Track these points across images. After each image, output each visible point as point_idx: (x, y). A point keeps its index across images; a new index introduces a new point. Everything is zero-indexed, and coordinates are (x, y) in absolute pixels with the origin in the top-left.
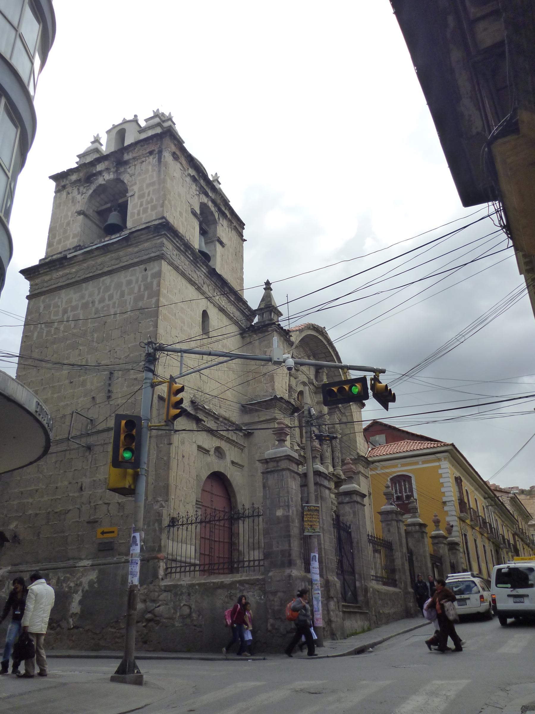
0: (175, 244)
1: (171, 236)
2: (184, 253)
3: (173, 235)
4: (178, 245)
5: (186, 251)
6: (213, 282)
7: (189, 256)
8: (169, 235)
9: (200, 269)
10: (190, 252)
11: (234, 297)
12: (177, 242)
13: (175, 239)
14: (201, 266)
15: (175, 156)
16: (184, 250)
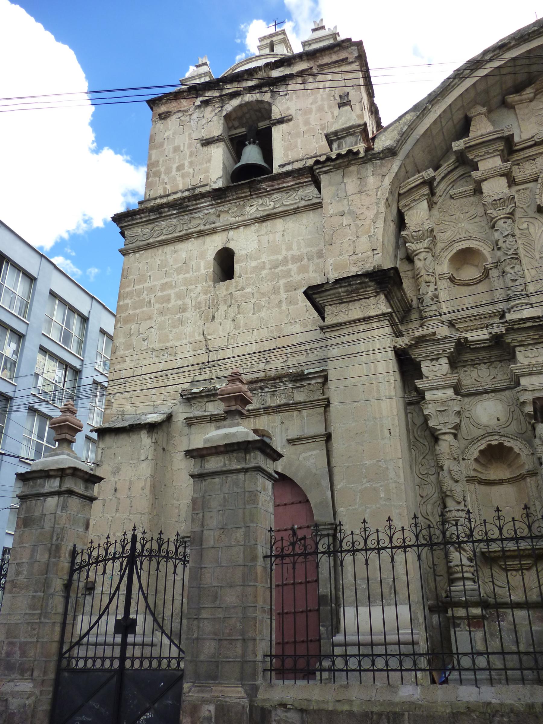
0: (142, 222)
1: (129, 221)
2: (161, 217)
3: (130, 218)
4: (145, 219)
5: (161, 213)
6: (234, 199)
7: (170, 213)
8: (125, 224)
9: (200, 208)
10: (166, 210)
11: (290, 179)
12: (141, 218)
13: (136, 219)
14: (197, 204)
15: (163, 116)
16: (158, 216)
